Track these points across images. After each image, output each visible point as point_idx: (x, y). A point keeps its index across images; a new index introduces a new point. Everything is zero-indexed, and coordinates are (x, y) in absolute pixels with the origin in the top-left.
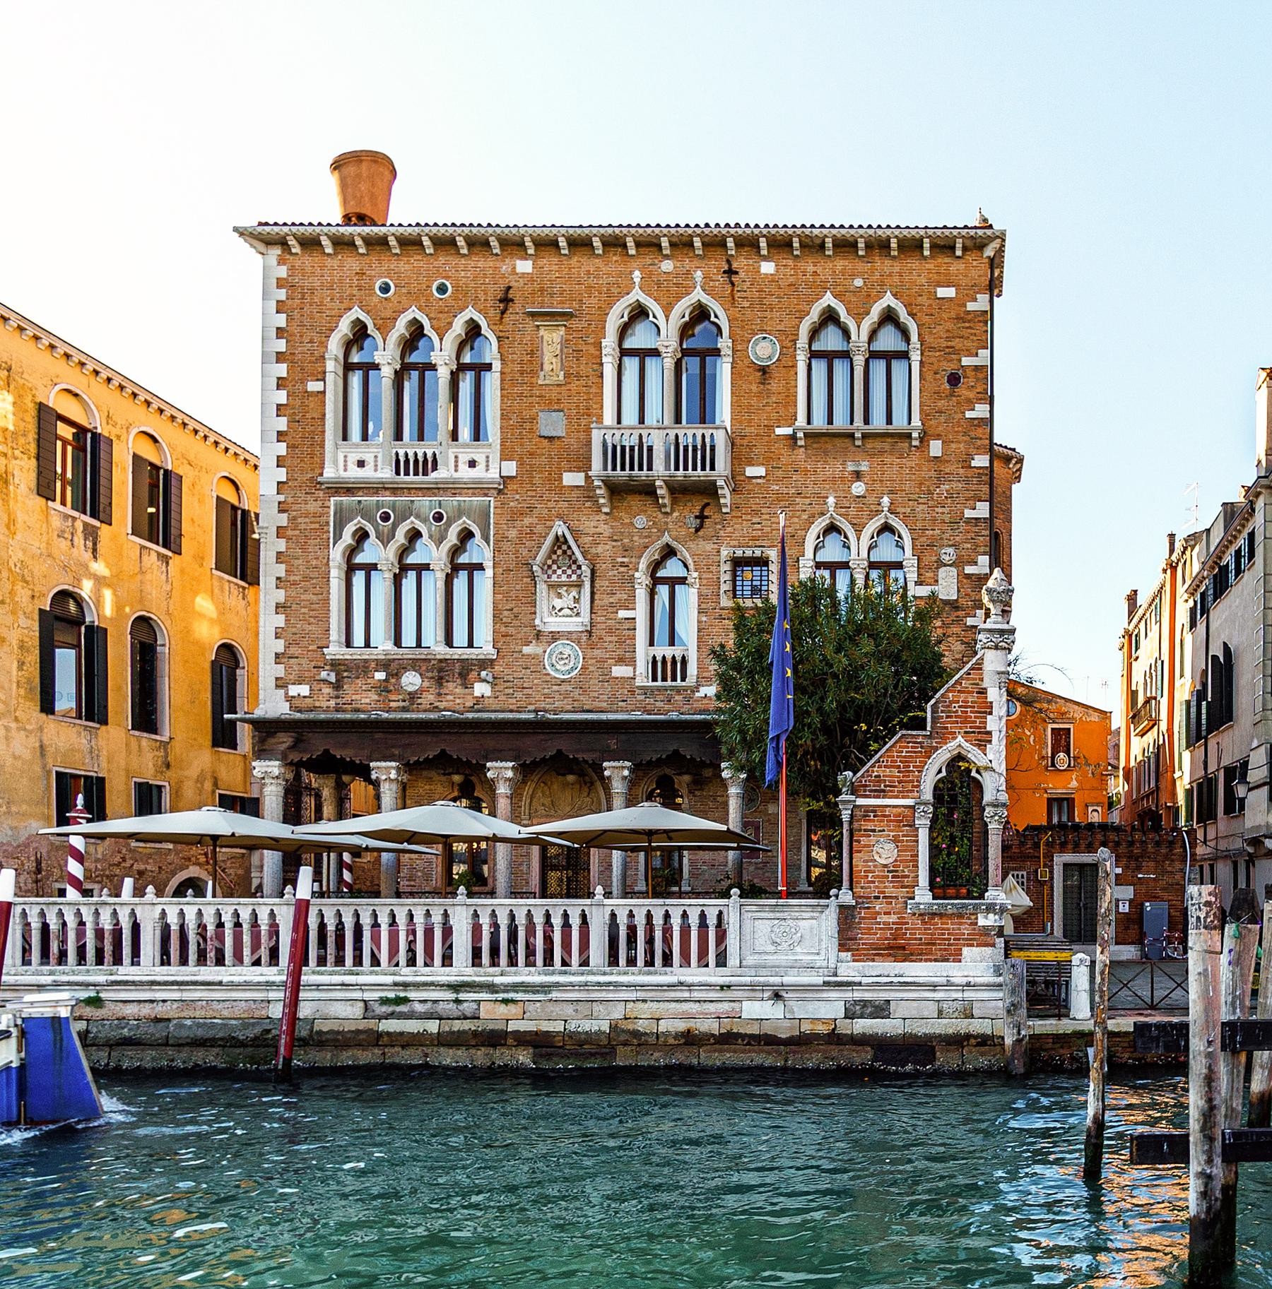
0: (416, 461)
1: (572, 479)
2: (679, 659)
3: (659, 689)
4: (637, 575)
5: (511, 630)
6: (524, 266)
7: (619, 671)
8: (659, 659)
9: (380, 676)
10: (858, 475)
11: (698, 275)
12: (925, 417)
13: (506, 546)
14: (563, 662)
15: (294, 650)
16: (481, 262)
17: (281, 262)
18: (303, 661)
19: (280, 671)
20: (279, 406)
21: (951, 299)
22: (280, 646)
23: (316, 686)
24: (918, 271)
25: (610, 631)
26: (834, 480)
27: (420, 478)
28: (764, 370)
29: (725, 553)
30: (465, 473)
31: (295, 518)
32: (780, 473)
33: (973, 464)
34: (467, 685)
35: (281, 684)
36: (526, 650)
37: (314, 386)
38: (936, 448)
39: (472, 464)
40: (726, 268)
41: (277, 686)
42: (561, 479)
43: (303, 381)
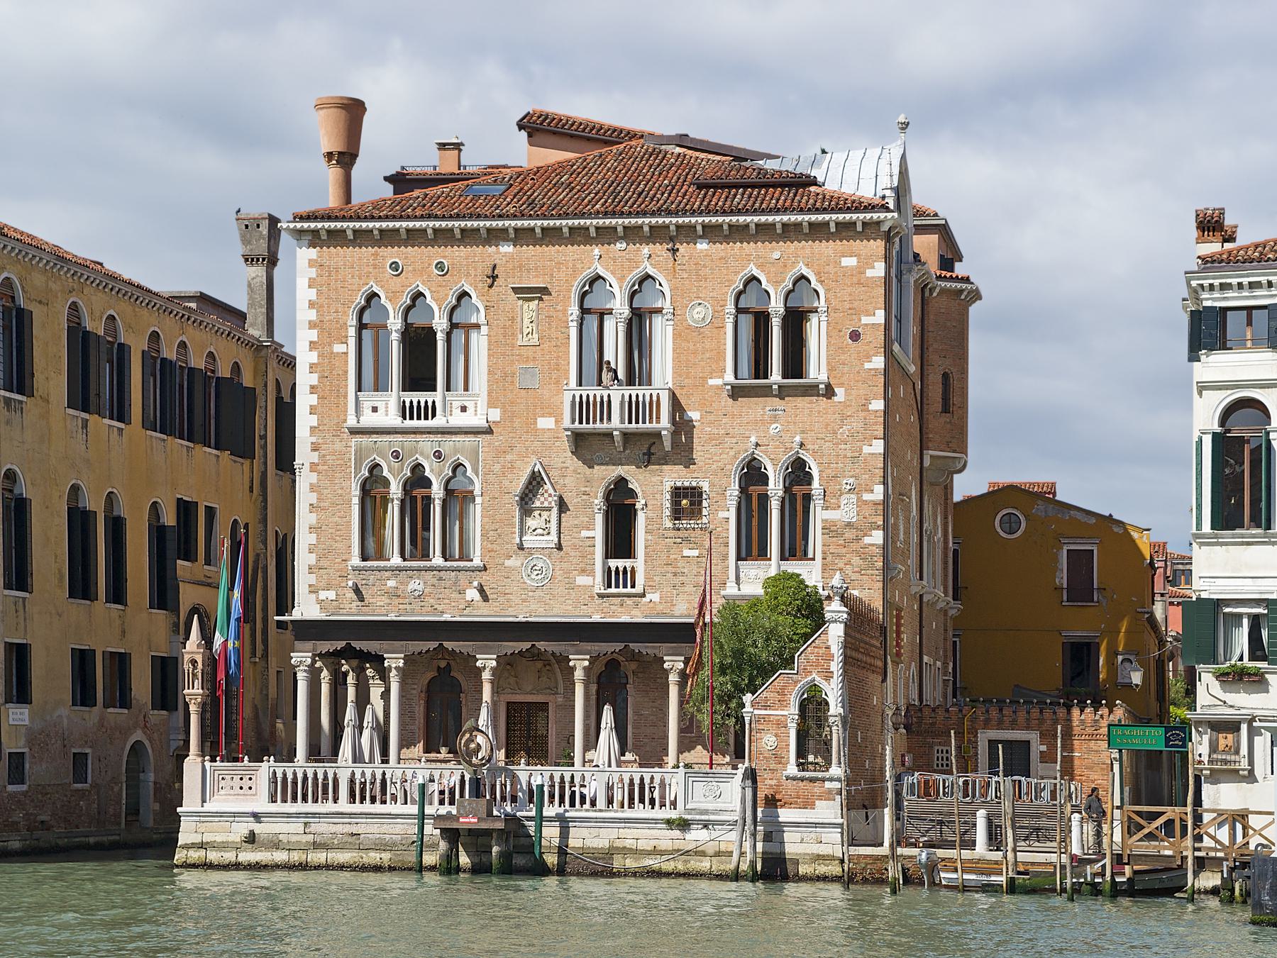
1: (546, 423)
2: (629, 569)
4: (596, 502)
6: (507, 249)
8: (613, 569)
10: (775, 419)
12: (831, 369)
13: (491, 478)
15: (324, 563)
19: (312, 579)
21: (852, 268)
22: (312, 559)
25: (575, 547)
26: (756, 422)
29: (668, 486)
30: (458, 420)
32: (712, 418)
33: (871, 407)
34: (462, 592)
35: (313, 590)
36: (507, 563)
37: (339, 348)
39: (464, 409)
40: (670, 246)
42: (535, 423)
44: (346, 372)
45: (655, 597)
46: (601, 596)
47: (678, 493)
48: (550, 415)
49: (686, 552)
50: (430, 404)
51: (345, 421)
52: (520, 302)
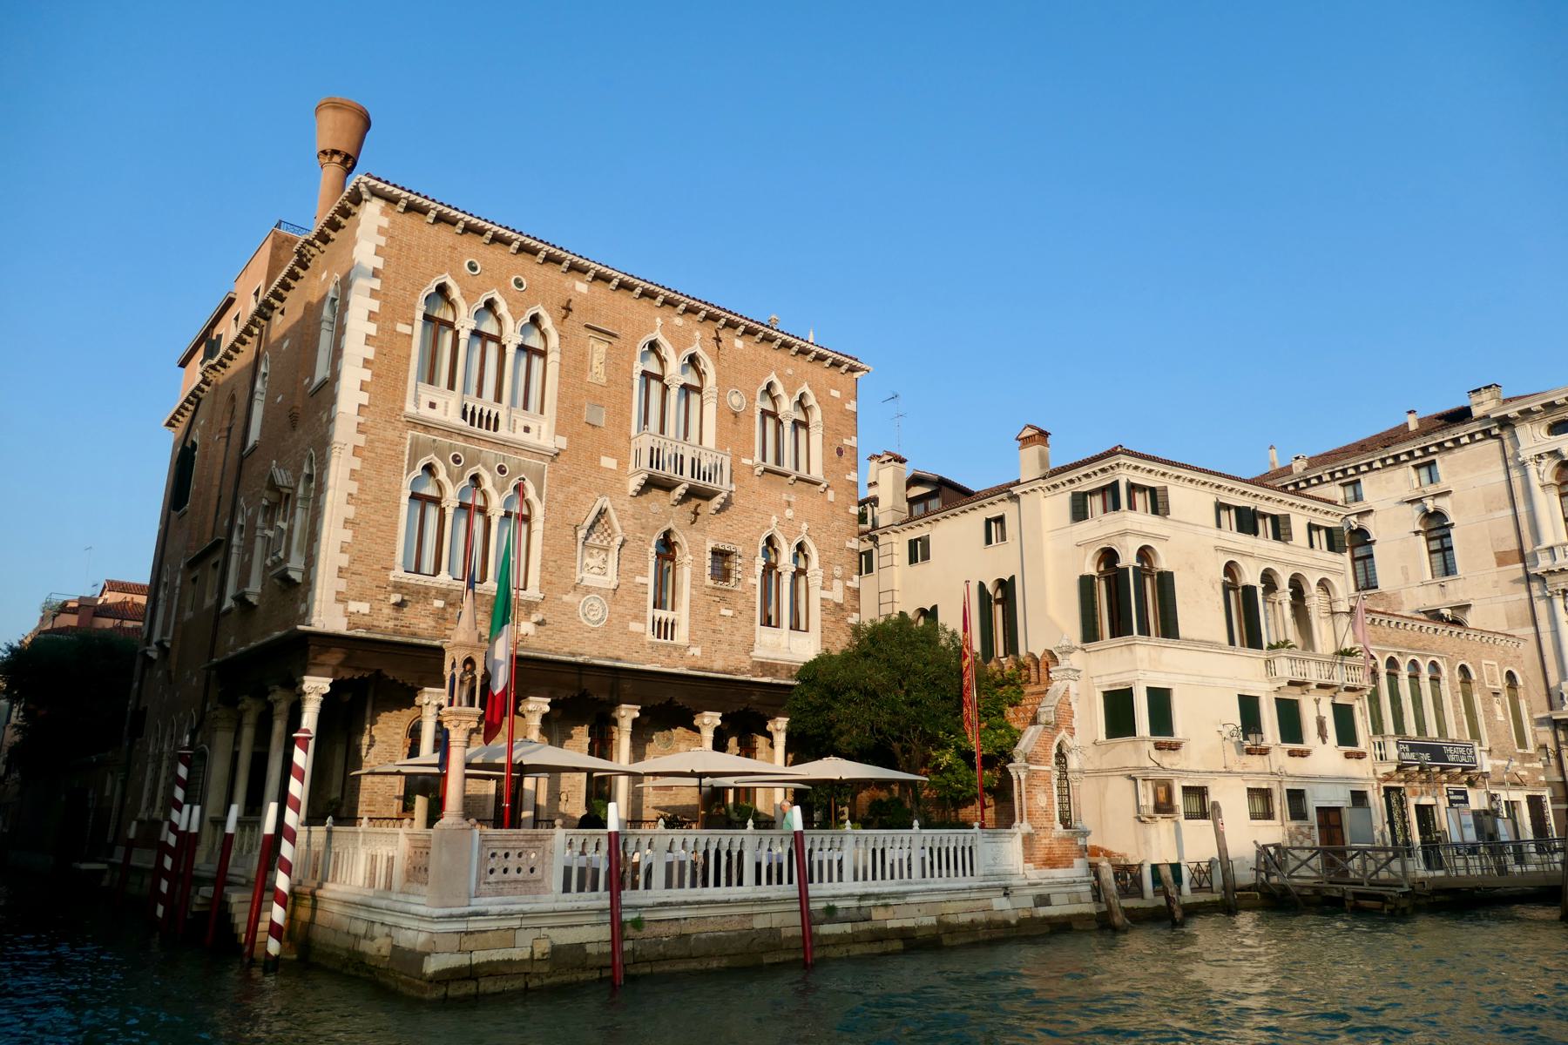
0: (489, 417)
1: (608, 462)
3: (662, 645)
5: (554, 579)
6: (581, 286)
7: (635, 627)
9: (439, 604)
10: (789, 504)
11: (697, 334)
12: (826, 473)
13: (554, 505)
14: (593, 612)
16: (553, 273)
17: (384, 213)
18: (366, 580)
19: (342, 585)
20: (368, 337)
22: (344, 560)
23: (376, 605)
24: (821, 372)
25: (629, 592)
27: (483, 431)
28: (736, 414)
29: (710, 545)
30: (520, 435)
31: (372, 441)
35: (341, 598)
36: (566, 598)
37: (402, 328)
38: (831, 495)
41: (337, 600)
43: (393, 321)
44: (409, 356)
45: (696, 651)
46: (653, 646)
47: (715, 552)
48: (613, 456)
49: (724, 612)
50: (493, 416)
51: (402, 409)
52: (592, 341)
